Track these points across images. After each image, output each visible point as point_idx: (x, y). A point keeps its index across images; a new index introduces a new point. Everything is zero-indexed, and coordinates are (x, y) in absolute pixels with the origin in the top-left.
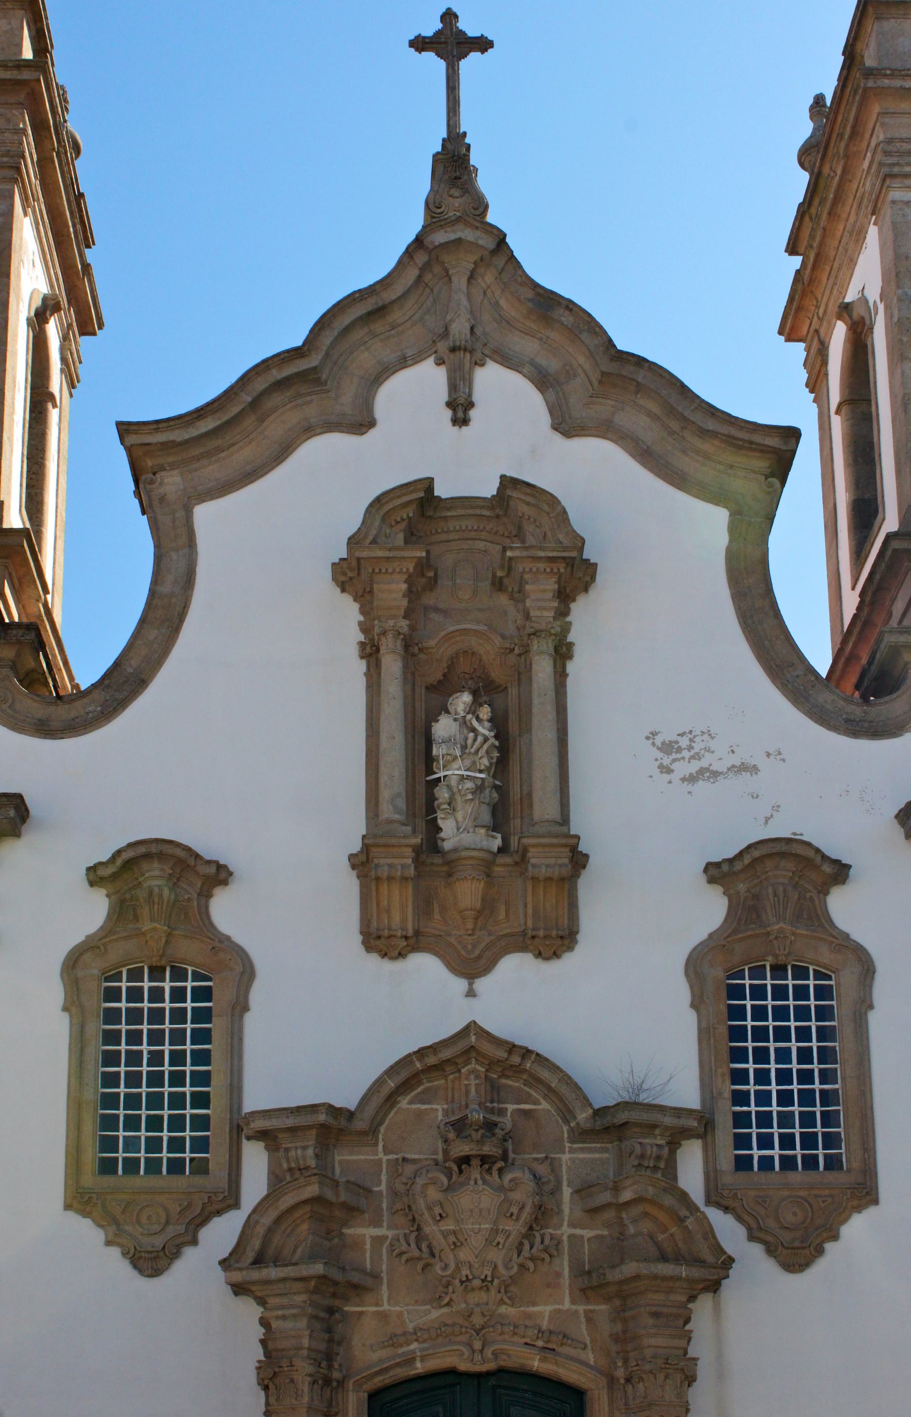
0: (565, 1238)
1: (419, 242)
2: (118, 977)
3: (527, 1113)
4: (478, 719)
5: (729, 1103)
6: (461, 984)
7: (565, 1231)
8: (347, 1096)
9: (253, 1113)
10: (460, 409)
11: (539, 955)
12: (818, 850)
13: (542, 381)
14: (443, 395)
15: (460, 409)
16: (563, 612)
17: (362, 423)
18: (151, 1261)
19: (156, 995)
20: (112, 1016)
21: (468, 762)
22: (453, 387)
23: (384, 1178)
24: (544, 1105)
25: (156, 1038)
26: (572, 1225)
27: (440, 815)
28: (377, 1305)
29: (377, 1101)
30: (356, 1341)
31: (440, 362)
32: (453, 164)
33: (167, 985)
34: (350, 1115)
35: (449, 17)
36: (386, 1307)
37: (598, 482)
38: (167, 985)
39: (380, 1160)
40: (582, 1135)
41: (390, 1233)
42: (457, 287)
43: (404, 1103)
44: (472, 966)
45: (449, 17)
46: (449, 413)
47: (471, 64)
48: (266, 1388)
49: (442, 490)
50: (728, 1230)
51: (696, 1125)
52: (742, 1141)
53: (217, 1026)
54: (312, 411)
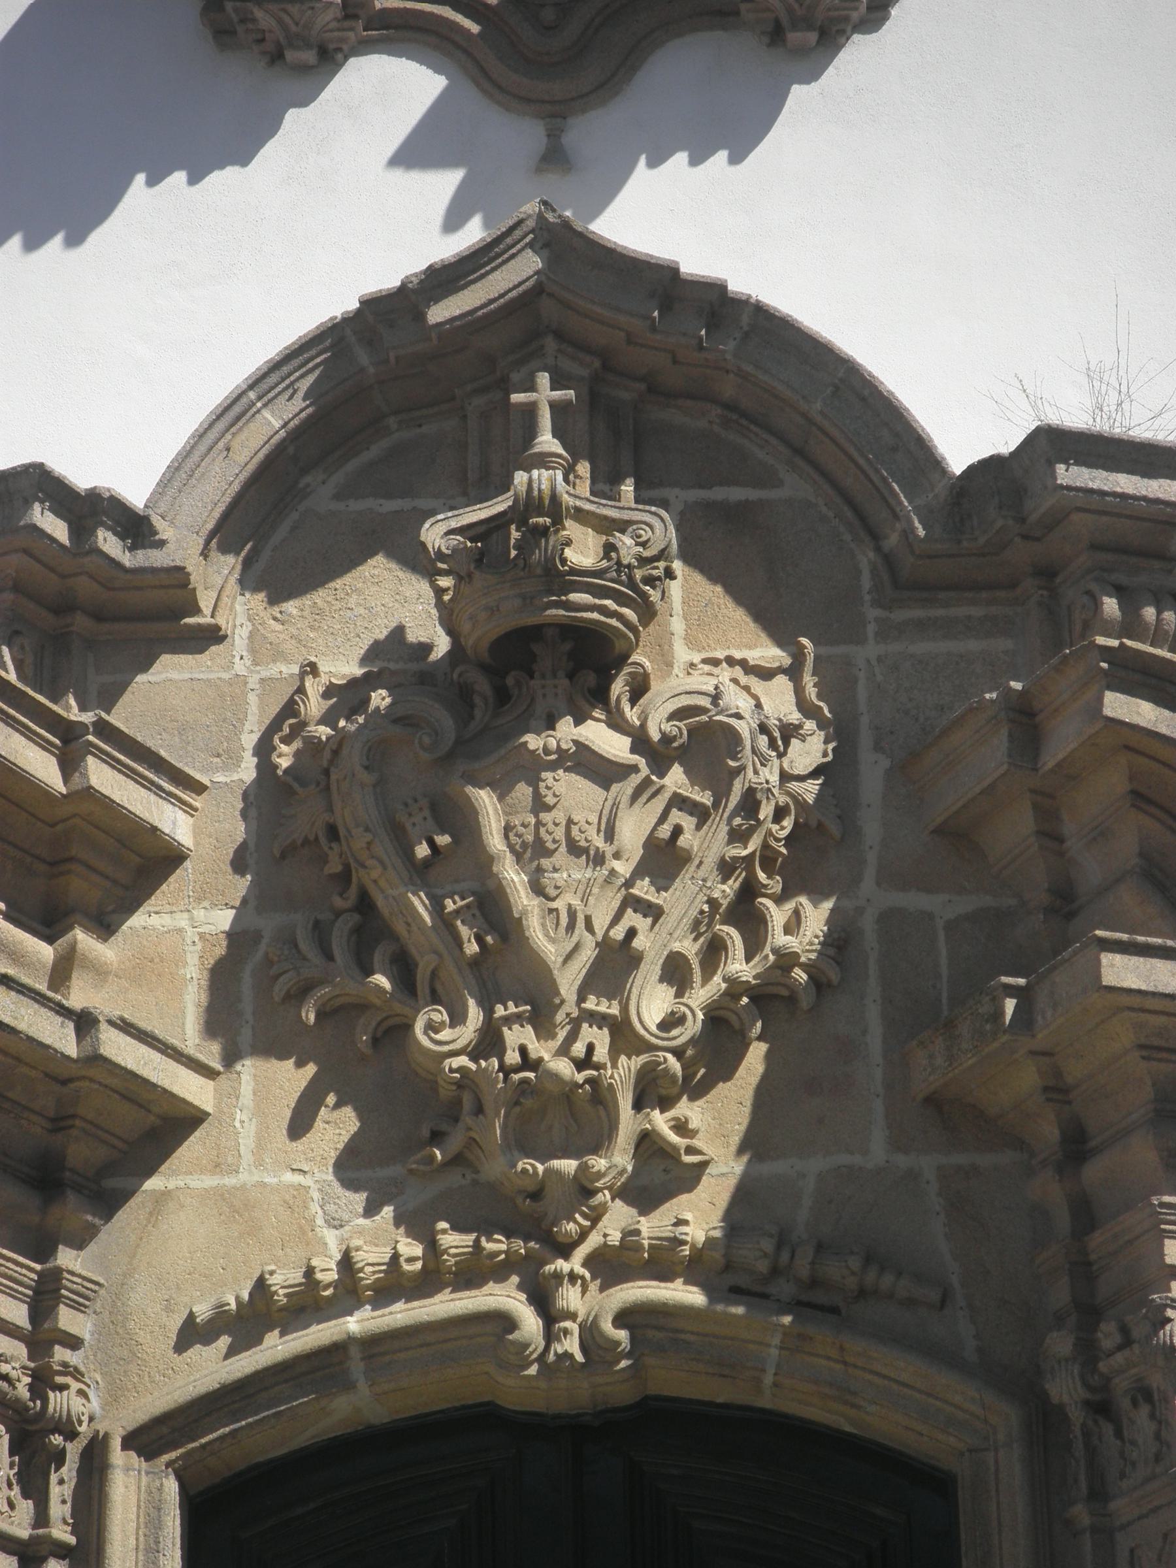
24: (794, 486)
28: (217, 1167)
34: (136, 527)
36: (246, 1176)
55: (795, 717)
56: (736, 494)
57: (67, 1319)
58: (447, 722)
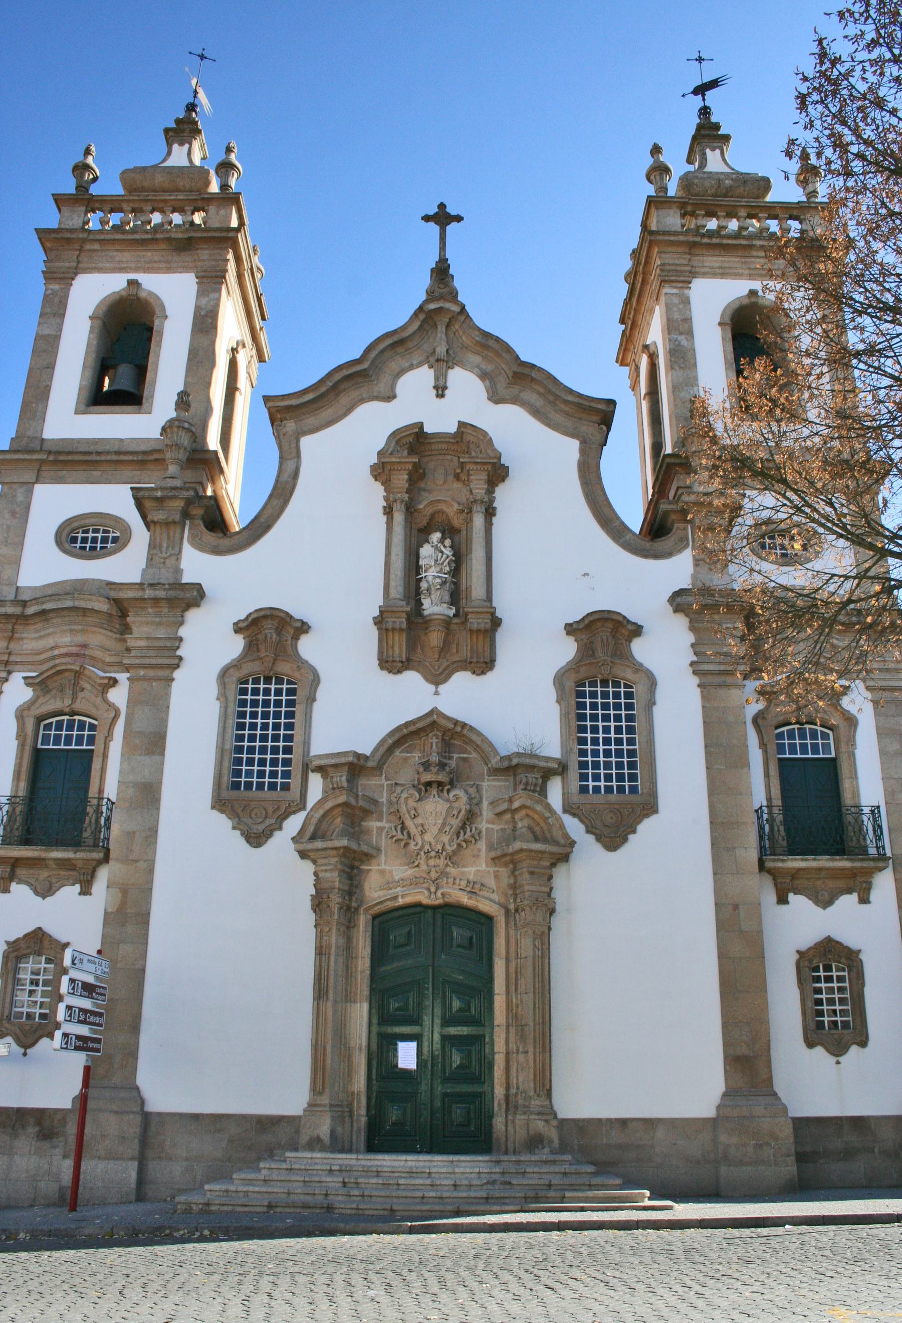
1: (421, 309)
2: (247, 682)
3: (465, 759)
4: (445, 546)
6: (432, 688)
8: (366, 748)
10: (440, 390)
11: (474, 673)
12: (625, 617)
13: (484, 376)
14: (433, 384)
15: (440, 390)
16: (490, 491)
17: (390, 397)
18: (256, 838)
19: (267, 692)
20: (243, 703)
21: (438, 569)
22: (437, 379)
23: (385, 794)
24: (474, 755)
25: (265, 715)
26: (488, 822)
27: (422, 596)
28: (378, 865)
29: (382, 750)
30: (367, 887)
31: (431, 367)
32: (442, 272)
33: (273, 687)
34: (367, 758)
35: (442, 206)
36: (383, 867)
37: (512, 428)
38: (273, 687)
40: (496, 772)
41: (387, 825)
42: (440, 327)
43: (397, 753)
44: (438, 678)
45: (442, 206)
46: (435, 392)
47: (452, 228)
48: (315, 912)
49: (428, 429)
50: (574, 827)
52: (583, 777)
53: (298, 710)
54: (364, 391)
58: (417, 795)
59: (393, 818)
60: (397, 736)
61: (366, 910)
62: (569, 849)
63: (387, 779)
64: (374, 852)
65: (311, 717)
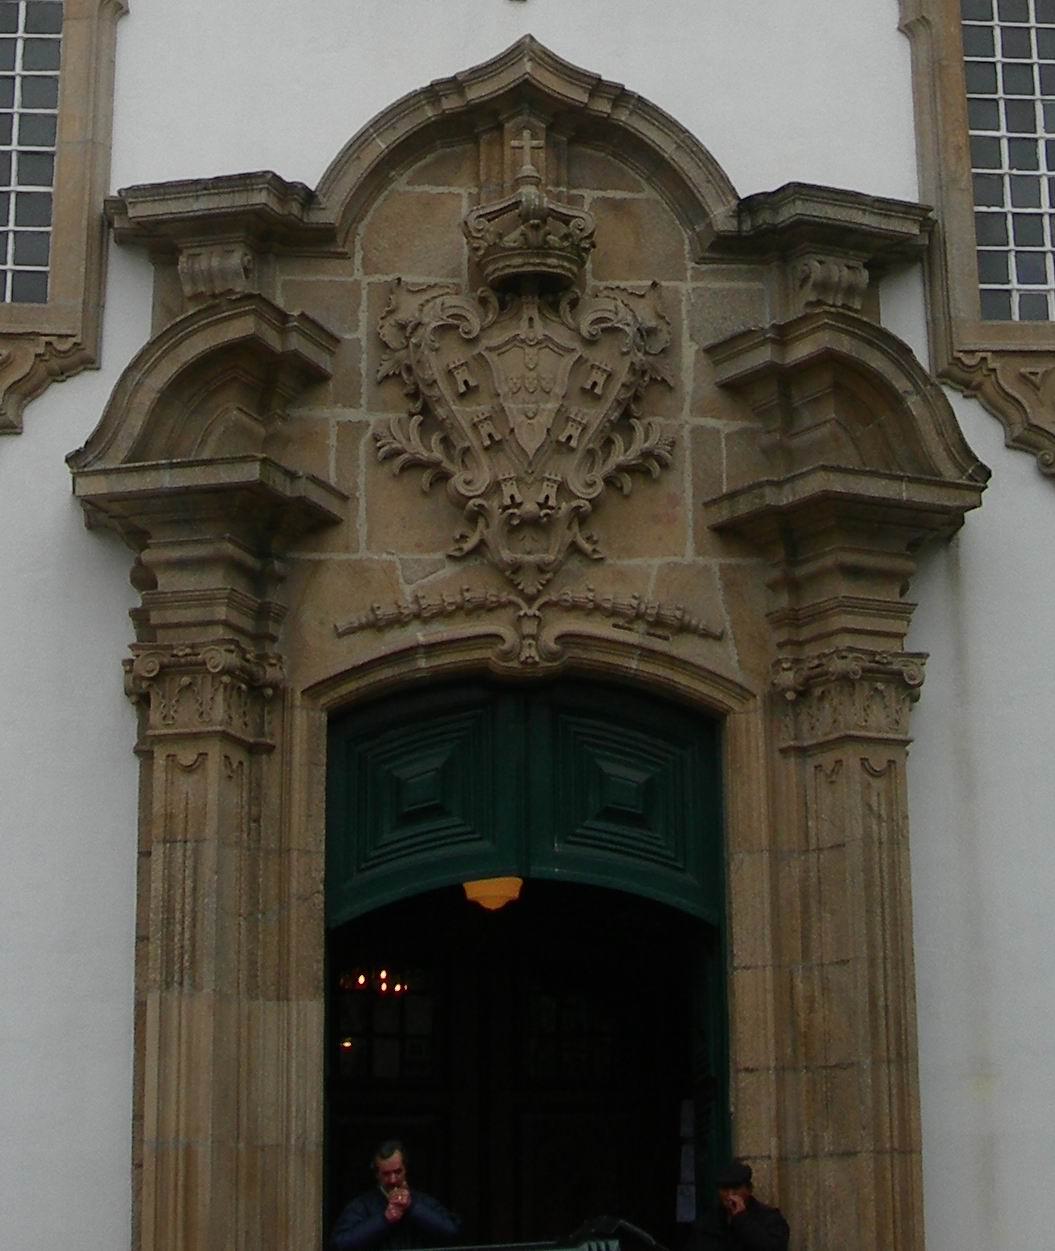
0: (686, 433)
3: (616, 206)
5: (968, 198)
7: (687, 420)
9: (135, 190)
26: (700, 410)
28: (347, 549)
34: (308, 197)
36: (362, 554)
39: (357, 283)
48: (141, 700)
51: (916, 231)
55: (653, 323)
56: (619, 195)
57: (272, 628)
59: (393, 392)
60: (403, 128)
61: (313, 691)
62: (970, 498)
63: (369, 267)
64: (333, 506)
65: (112, 62)
